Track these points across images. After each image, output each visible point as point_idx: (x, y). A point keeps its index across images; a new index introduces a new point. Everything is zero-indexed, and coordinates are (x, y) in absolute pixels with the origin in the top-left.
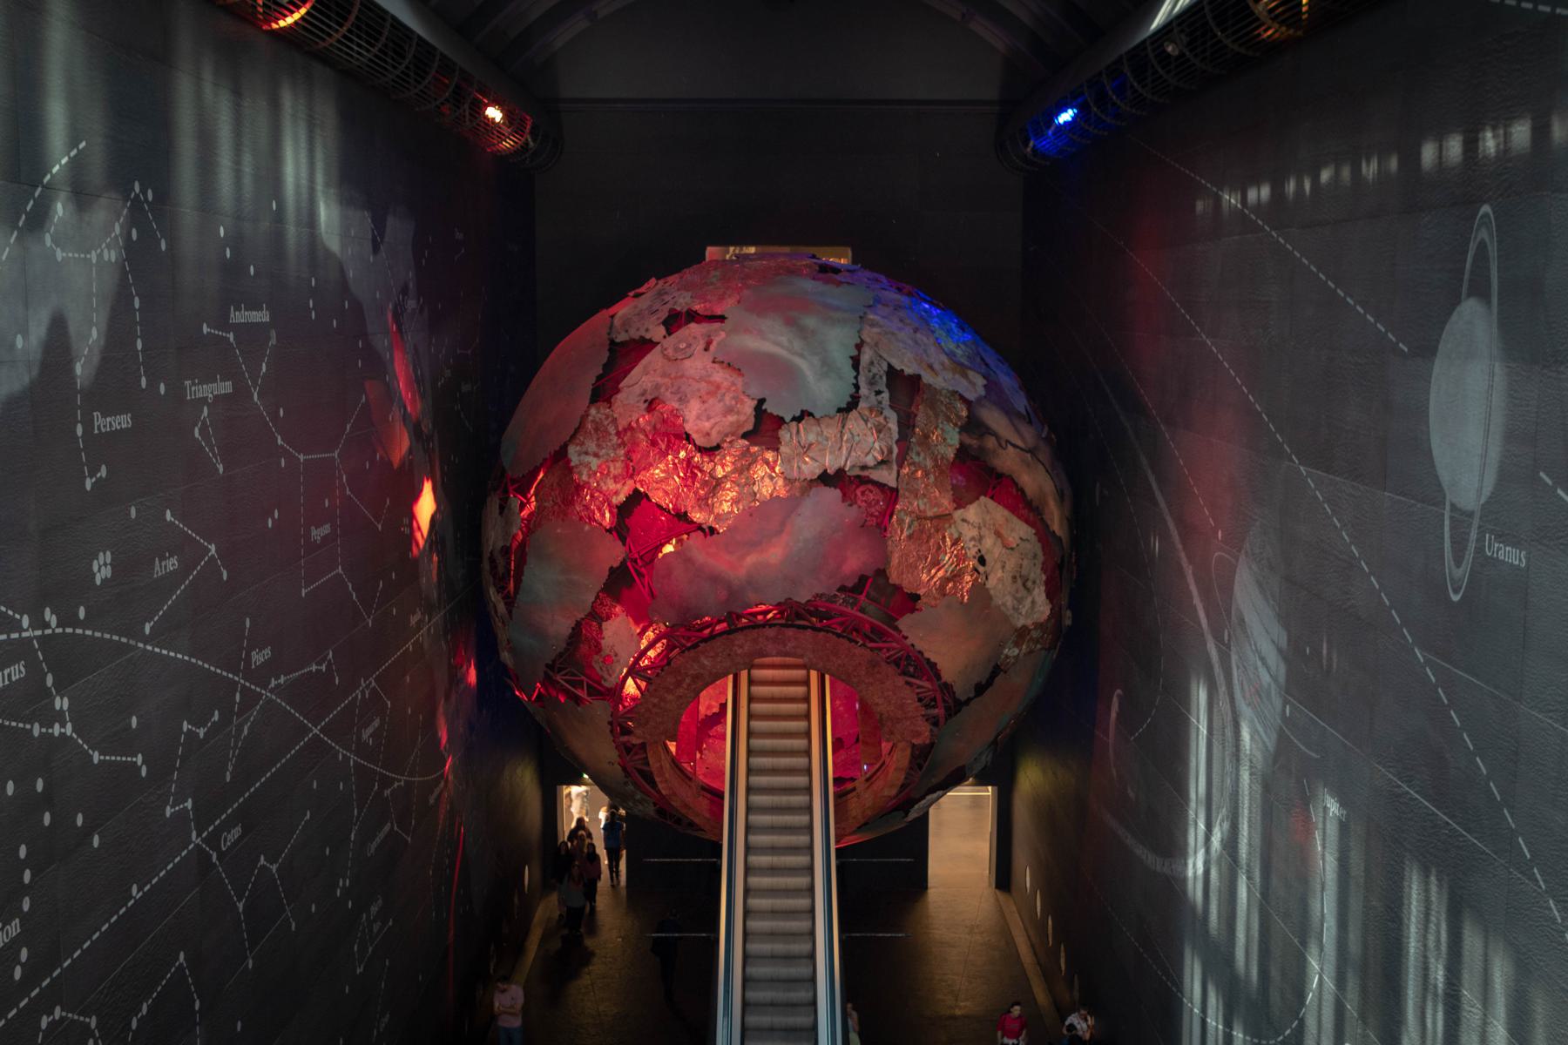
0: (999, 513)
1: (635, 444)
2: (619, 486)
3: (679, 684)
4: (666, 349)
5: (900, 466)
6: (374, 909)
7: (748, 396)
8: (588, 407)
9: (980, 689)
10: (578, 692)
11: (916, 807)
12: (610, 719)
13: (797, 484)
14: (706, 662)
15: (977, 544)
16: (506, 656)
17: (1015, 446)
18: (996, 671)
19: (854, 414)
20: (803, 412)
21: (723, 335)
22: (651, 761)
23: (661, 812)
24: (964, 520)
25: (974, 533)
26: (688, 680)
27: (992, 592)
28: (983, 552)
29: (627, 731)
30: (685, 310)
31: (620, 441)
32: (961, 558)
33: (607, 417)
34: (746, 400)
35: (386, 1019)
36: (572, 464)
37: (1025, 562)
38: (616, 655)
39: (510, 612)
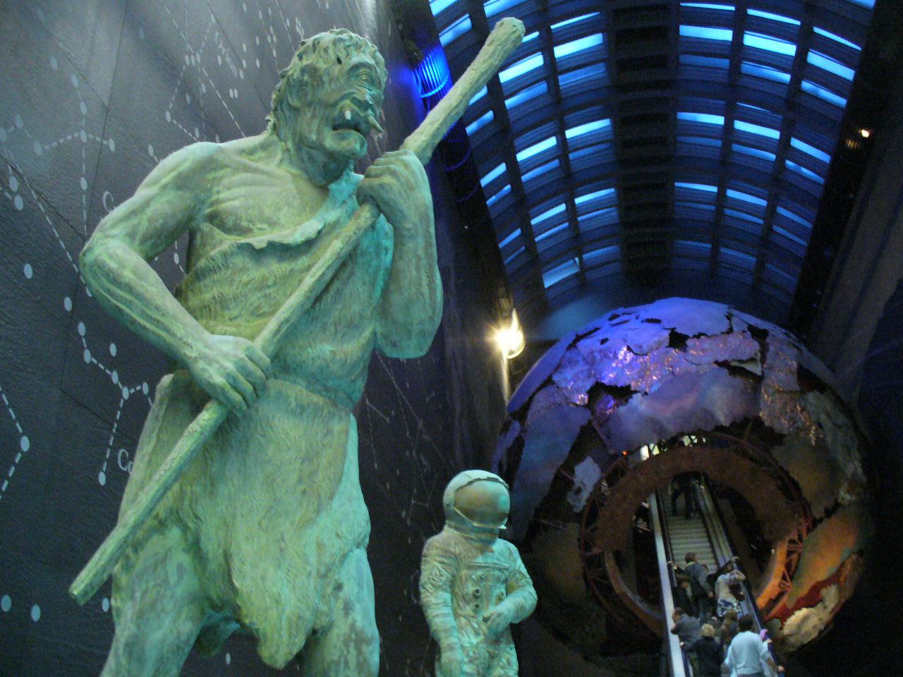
38: (584, 485)
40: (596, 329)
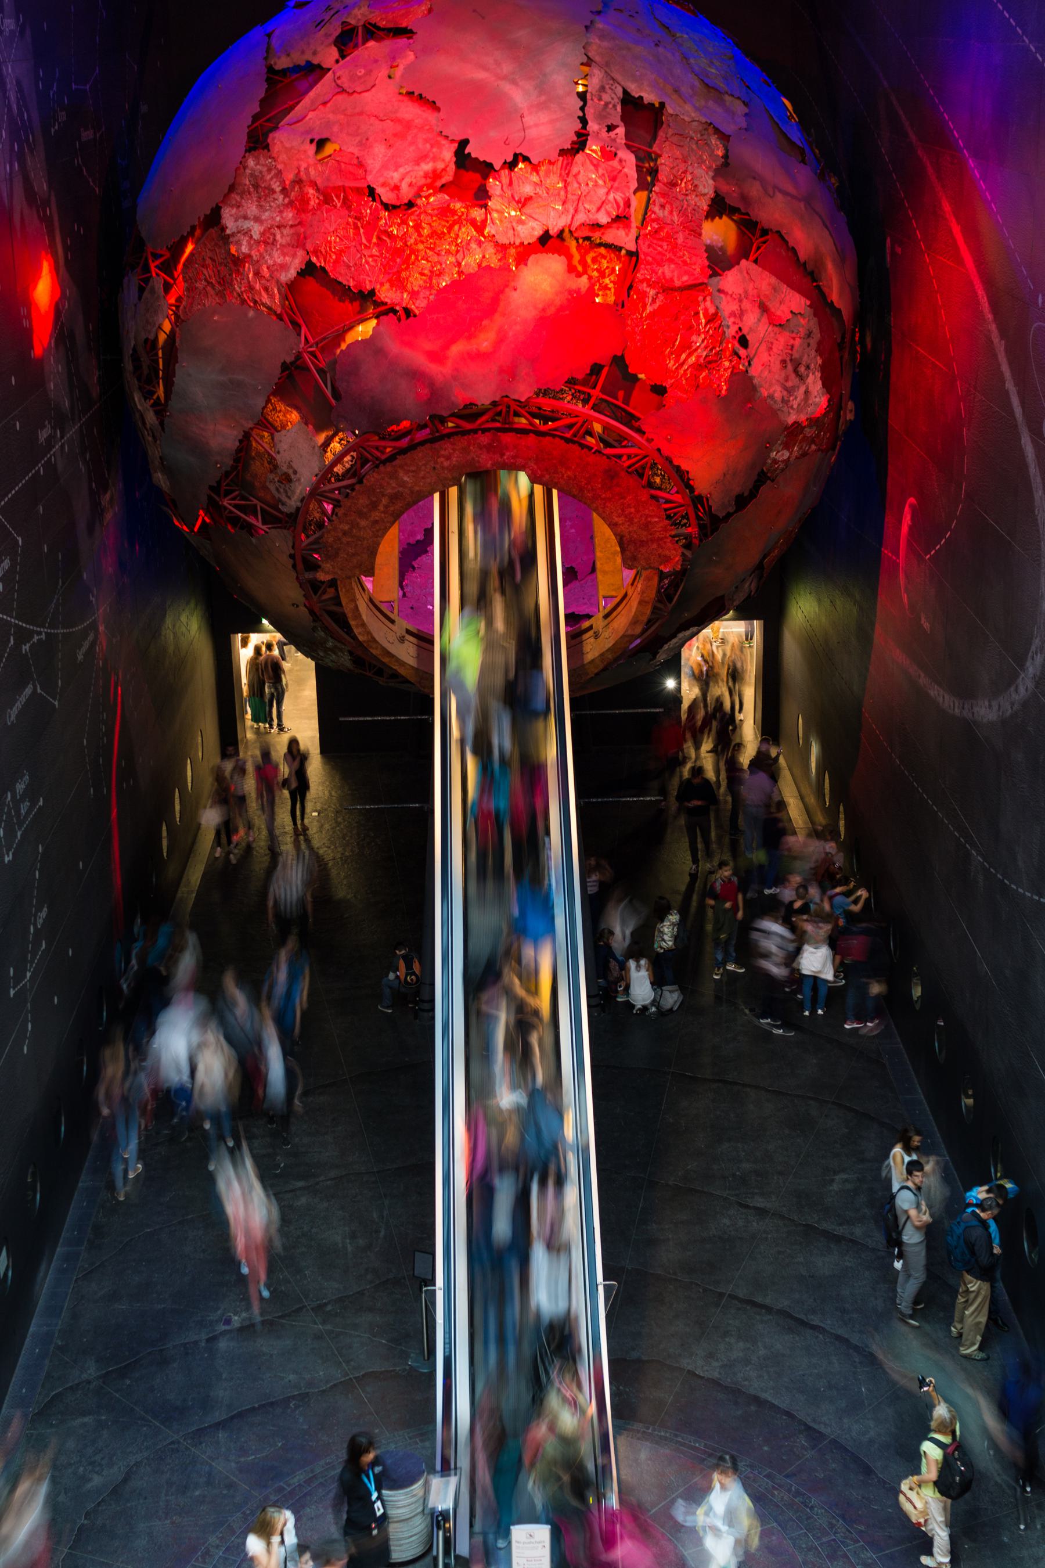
0: (764, 281)
1: (304, 200)
3: (374, 506)
4: (339, 78)
6: (20, 787)
7: (447, 137)
8: (244, 157)
9: (742, 502)
10: (251, 520)
11: (666, 647)
12: (292, 552)
13: (513, 251)
14: (406, 479)
15: (738, 320)
16: (160, 478)
17: (785, 193)
18: (762, 478)
19: (579, 157)
20: (516, 156)
21: (411, 56)
22: (344, 601)
23: (358, 661)
24: (720, 291)
25: (734, 307)
26: (384, 501)
27: (756, 381)
28: (745, 332)
29: (314, 567)
30: (361, 23)
31: (287, 201)
32: (717, 337)
33: (269, 170)
34: (444, 142)
35: (43, 914)
36: (228, 232)
37: (797, 342)
38: (295, 472)
39: (162, 424)
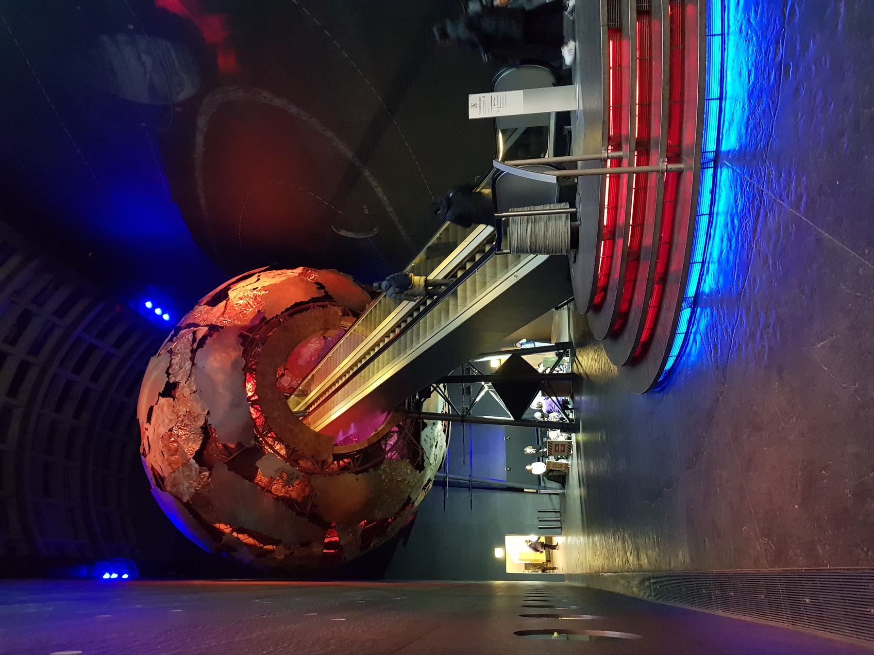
2: (193, 469)
5: (198, 325)
14: (277, 414)
40: (152, 468)
